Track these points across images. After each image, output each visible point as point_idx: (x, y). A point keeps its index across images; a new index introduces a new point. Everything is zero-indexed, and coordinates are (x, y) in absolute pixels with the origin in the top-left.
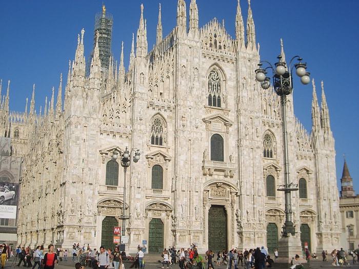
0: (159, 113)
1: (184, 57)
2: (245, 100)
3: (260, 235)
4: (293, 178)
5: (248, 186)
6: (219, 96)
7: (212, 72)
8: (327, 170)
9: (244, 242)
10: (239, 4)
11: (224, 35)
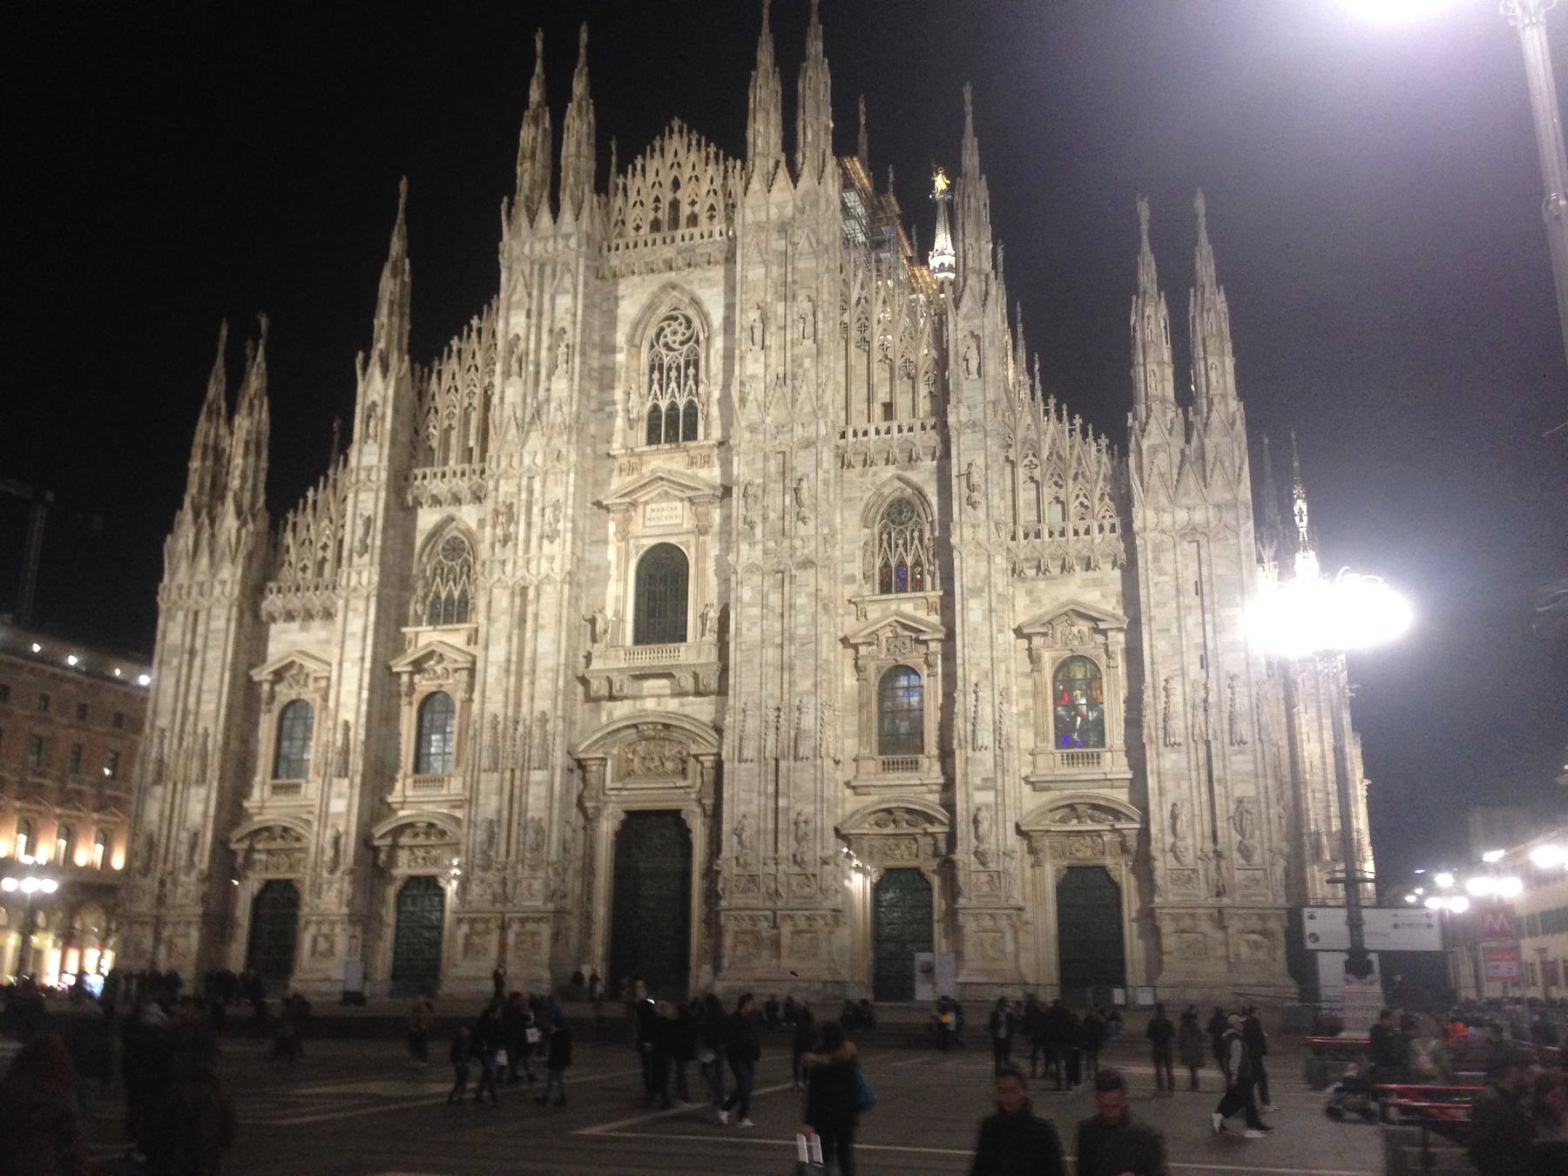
0: (451, 519)
1: (519, 305)
2: (756, 391)
3: (803, 924)
4: (986, 665)
5: (752, 725)
6: (691, 406)
7: (665, 324)
8: (1191, 599)
9: (727, 952)
10: (766, 23)
11: (711, 169)
